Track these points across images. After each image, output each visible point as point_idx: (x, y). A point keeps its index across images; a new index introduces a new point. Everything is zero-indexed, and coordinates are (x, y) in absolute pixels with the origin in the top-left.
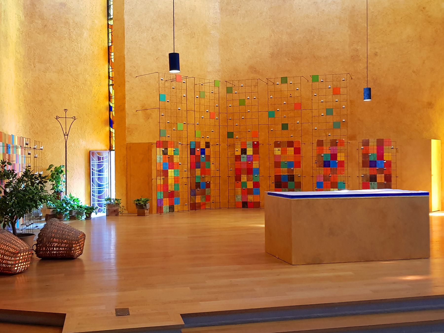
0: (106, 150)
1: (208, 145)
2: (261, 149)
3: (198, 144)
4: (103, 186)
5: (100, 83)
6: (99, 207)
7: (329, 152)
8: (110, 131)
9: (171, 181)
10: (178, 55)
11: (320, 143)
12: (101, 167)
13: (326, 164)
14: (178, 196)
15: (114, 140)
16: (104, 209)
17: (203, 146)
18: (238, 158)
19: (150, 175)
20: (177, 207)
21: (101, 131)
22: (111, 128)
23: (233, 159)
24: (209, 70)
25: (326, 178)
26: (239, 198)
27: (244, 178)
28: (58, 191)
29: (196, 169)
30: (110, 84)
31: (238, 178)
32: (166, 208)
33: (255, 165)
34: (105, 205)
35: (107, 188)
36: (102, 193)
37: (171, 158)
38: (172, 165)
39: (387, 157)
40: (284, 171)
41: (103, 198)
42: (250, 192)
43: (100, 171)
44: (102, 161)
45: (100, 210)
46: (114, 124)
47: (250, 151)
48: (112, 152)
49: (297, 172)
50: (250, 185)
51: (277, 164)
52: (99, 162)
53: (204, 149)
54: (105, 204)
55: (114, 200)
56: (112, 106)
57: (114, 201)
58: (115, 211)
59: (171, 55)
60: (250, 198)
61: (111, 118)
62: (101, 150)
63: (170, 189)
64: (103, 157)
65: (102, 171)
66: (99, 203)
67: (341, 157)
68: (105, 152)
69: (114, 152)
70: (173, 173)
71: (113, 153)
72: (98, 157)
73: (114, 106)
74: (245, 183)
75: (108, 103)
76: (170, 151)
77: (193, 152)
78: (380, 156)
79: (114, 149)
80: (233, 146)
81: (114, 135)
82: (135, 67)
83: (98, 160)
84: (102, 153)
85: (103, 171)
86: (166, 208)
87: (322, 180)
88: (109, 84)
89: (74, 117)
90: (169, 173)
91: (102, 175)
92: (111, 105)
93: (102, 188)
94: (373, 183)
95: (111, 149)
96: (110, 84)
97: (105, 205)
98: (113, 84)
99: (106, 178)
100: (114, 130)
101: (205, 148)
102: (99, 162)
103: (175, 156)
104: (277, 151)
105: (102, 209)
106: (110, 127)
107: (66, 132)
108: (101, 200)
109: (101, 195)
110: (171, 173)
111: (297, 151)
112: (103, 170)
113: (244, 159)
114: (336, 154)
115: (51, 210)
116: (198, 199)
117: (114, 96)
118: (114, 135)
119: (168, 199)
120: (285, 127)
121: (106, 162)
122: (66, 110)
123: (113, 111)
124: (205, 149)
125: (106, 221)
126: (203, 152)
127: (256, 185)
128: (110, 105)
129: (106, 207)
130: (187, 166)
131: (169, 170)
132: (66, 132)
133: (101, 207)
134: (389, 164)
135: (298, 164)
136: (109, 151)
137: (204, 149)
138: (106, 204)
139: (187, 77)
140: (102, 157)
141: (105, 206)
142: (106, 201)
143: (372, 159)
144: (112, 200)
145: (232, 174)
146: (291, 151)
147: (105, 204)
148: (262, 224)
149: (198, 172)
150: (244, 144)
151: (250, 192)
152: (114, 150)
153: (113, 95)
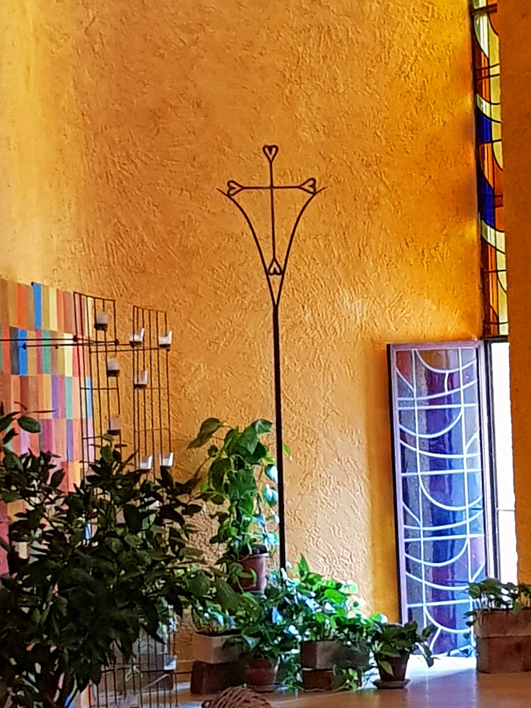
0: (467, 339)
4: (455, 522)
5: (431, 6)
6: (440, 627)
8: (484, 244)
12: (446, 423)
15: (505, 288)
16: (467, 636)
21: (441, 244)
22: (489, 228)
28: (246, 547)
30: (478, 5)
34: (471, 619)
35: (474, 530)
36: (451, 558)
41: (456, 578)
43: (441, 446)
44: (447, 393)
45: (446, 642)
46: (502, 206)
48: (495, 346)
52: (431, 402)
54: (469, 614)
55: (512, 591)
56: (488, 114)
57: (514, 597)
58: (519, 647)
61: (488, 174)
62: (443, 341)
64: (451, 375)
65: (447, 442)
66: (439, 608)
68: (460, 348)
69: (507, 345)
72: (430, 375)
73: (502, 118)
75: (469, 102)
79: (504, 330)
81: (501, 259)
83: (431, 392)
84: (447, 356)
85: (453, 444)
88: (471, 7)
89: (311, 182)
91: (451, 468)
92: (486, 109)
93: (452, 532)
95: (489, 330)
96: (475, 7)
97: (471, 619)
98: (496, 5)
99: (471, 476)
100: (501, 236)
102: (431, 402)
105: (456, 635)
106: (483, 221)
107: (274, 259)
108: (447, 591)
109: (447, 566)
112: (453, 439)
115: (218, 642)
117: (498, 68)
118: (501, 259)
121: (465, 403)
122: (274, 150)
123: (494, 139)
125: (474, 700)
128: (478, 112)
129: (472, 627)
132: (274, 259)
133: (452, 624)
136: (481, 343)
138: (474, 613)
140: (447, 372)
141: (469, 624)
142: (476, 596)
144: (504, 591)
147: (471, 609)
152: (504, 339)
153: (495, 59)
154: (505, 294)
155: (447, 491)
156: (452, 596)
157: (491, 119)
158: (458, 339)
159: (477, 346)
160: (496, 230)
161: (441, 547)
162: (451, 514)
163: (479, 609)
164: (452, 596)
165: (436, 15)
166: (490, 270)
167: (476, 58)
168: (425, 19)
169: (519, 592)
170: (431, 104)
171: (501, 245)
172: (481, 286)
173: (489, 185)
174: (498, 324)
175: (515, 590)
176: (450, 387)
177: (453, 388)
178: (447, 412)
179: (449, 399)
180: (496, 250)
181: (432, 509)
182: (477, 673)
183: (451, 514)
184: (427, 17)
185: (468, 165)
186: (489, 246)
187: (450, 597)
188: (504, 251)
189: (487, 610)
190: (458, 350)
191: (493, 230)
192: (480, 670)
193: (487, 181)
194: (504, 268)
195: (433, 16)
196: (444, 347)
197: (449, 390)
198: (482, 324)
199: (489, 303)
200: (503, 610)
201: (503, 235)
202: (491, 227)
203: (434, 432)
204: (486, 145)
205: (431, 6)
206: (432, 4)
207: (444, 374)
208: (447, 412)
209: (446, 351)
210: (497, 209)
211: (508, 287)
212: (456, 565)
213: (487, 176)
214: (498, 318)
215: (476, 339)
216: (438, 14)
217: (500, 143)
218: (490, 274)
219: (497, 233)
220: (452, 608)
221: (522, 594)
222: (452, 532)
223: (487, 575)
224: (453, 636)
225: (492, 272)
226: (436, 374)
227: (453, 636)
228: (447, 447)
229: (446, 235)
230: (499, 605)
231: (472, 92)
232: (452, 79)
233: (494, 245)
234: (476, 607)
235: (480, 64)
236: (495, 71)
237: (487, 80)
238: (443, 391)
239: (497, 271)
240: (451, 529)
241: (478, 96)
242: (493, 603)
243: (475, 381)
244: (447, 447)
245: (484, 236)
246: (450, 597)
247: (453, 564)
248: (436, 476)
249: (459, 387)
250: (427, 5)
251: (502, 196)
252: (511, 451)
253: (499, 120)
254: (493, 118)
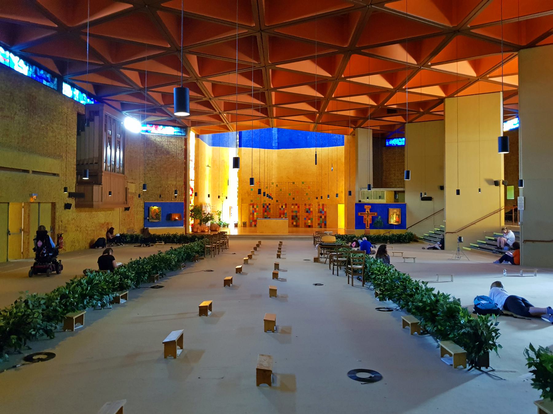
2: (288, 206)
11: (305, 205)
13: (307, 212)
17: (268, 205)
18: (280, 209)
33: (286, 211)
39: (325, 210)
40: (294, 214)
47: (284, 207)
51: (292, 212)
67: (311, 210)
77: (264, 207)
78: (323, 210)
80: (278, 205)
104: (293, 207)
113: (282, 209)
120: (294, 199)
126: (268, 207)
134: (325, 212)
135: (299, 212)
143: (321, 210)
146: (296, 207)
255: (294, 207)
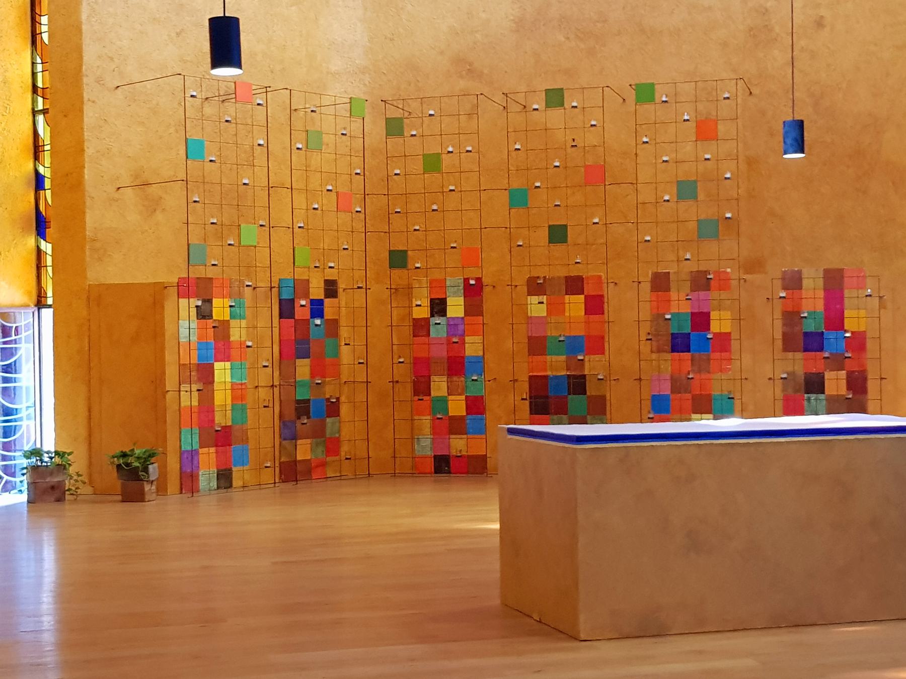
0: (26, 306)
1: (331, 289)
2: (490, 301)
3: (302, 287)
4: (16, 414)
5: (8, 107)
6: (6, 478)
7: (686, 309)
8: (39, 251)
9: (222, 397)
10: (235, 21)
11: (661, 283)
12: (12, 355)
13: (680, 343)
14: (245, 440)
15: (51, 277)
16: (21, 482)
17: (317, 291)
18: (421, 327)
19: (158, 381)
20: (239, 475)
21: (12, 249)
22: (42, 240)
23: (407, 330)
24: (333, 68)
25: (678, 386)
26: (425, 446)
27: (439, 386)
29: (297, 360)
30: (38, 108)
31: (421, 388)
32: (207, 477)
33: (472, 347)
34: (25, 471)
35: (28, 418)
36: (14, 435)
37: (222, 329)
38: (224, 350)
39: (854, 320)
41: (17, 448)
42: (456, 426)
43: (10, 369)
44: (13, 337)
45: (9, 486)
46: (50, 228)
47: (456, 307)
48: (44, 311)
49: (593, 365)
50: (457, 407)
52: (5, 343)
53: (320, 302)
54: (23, 469)
55: (50, 455)
56: (43, 174)
57: (51, 458)
58: (53, 488)
59: (214, 22)
60: (458, 445)
61: (42, 208)
62: (12, 306)
63: (221, 419)
64: (16, 327)
65: (13, 367)
66: (6, 465)
67: (720, 323)
68: (22, 311)
69: (51, 310)
70: (228, 372)
71: (47, 314)
72: (4, 326)
73: (51, 176)
74: (444, 401)
75: (30, 165)
76: (220, 308)
77: (286, 309)
78: (835, 321)
79: (50, 301)
80: (405, 292)
81: (49, 261)
82: (112, 59)
83: (4, 337)
84: (14, 315)
85: (17, 369)
86: (207, 477)
87: (666, 388)
88: (33, 109)
90: (216, 372)
91: (15, 382)
92: (41, 170)
93: (15, 420)
94: (813, 397)
95: (41, 301)
96: (36, 109)
97: (25, 471)
98: (48, 109)
99: (27, 388)
100: (49, 246)
101: (322, 297)
102: (5, 343)
103: (233, 323)
104: (537, 307)
105: (15, 482)
106: (39, 237)
108: (11, 456)
109: (11, 441)
110: (223, 372)
111: (595, 305)
112: (17, 365)
113: (439, 329)
114: (708, 315)
116: (304, 450)
117: (49, 146)
118: (49, 261)
119: (213, 450)
120: (558, 234)
121: (25, 342)
123: (46, 188)
124: (322, 300)
125: (25, 519)
126: (317, 309)
127: (476, 406)
128: (37, 173)
129: (25, 476)
130: (269, 351)
131: (218, 366)
133: (13, 475)
134: (858, 342)
135: (596, 345)
136: (36, 309)
137: (320, 302)
138: (26, 468)
139: (270, 87)
140: (14, 325)
141: (23, 475)
142: (28, 458)
143: (810, 326)
144: (46, 455)
145: (404, 373)
146: (575, 304)
147: (25, 466)
148: (492, 521)
149: (303, 368)
150: (438, 285)
151: (456, 426)
152: (50, 306)
153: (47, 141)
154: (51, 280)
155: (13, 396)
156: (14, 458)
157: (45, 177)
158: (22, 306)
159: (33, 310)
160: (47, 242)
161: (7, 429)
162: (15, 410)
163: (30, 466)
164: (14, 458)
165: (11, 112)
166: (42, 265)
167: (37, 139)
168: (5, 114)
169: (55, 455)
170: (7, 165)
171: (49, 251)
172: (37, 275)
173: (43, 216)
174: (46, 297)
175: (52, 454)
176: (16, 334)
177: (18, 335)
178: (14, 349)
179: (15, 341)
180: (46, 254)
181: (3, 408)
182: (27, 504)
183: (15, 410)
184: (6, 112)
185: (30, 202)
186: (42, 252)
187: (13, 459)
188: (51, 254)
189: (34, 466)
190: (21, 312)
191: (44, 242)
192: (29, 502)
193: (41, 213)
194: (51, 265)
195: (9, 113)
196: (12, 311)
197: (15, 335)
198: (36, 297)
199: (41, 284)
200: (44, 466)
201: (50, 245)
202: (44, 240)
203: (6, 360)
204: (41, 192)
205: (8, 107)
206: (10, 105)
207: (12, 327)
208: (14, 349)
209: (14, 312)
210: (47, 230)
211: (53, 276)
212: (17, 440)
213: (41, 210)
214: (46, 294)
215: (33, 306)
216: (13, 111)
217: (50, 191)
218: (42, 268)
219: (47, 243)
220: (13, 466)
221: (57, 456)
222: (15, 420)
223: (36, 445)
224: (14, 483)
225: (44, 267)
226: (7, 326)
227: (14, 483)
228: (14, 369)
229: (16, 243)
230: (42, 463)
231: (34, 160)
232: (21, 151)
233: (45, 250)
234: (28, 465)
235: (39, 143)
236: (47, 148)
237: (43, 153)
238: (11, 336)
239: (46, 266)
240: (15, 419)
241: (37, 162)
242: (38, 461)
243: (32, 331)
244: (14, 369)
245: (39, 245)
246: (13, 459)
247: (15, 440)
248: (6, 387)
249: (21, 334)
250: (6, 106)
251: (50, 222)
252: (53, 372)
253: (50, 177)
254: (46, 176)
255: (555, 308)
